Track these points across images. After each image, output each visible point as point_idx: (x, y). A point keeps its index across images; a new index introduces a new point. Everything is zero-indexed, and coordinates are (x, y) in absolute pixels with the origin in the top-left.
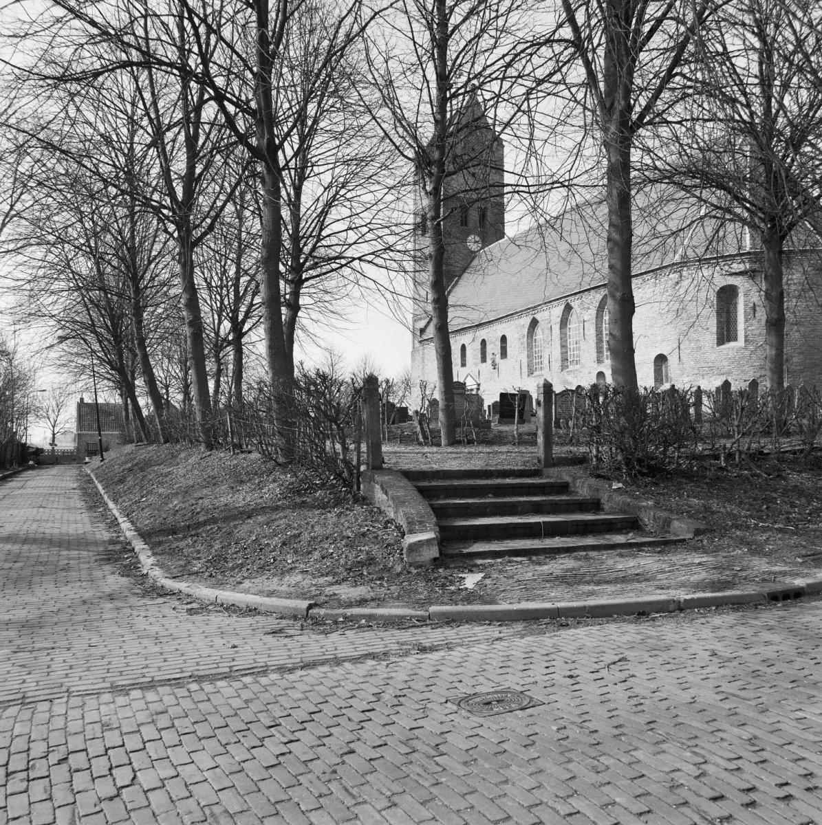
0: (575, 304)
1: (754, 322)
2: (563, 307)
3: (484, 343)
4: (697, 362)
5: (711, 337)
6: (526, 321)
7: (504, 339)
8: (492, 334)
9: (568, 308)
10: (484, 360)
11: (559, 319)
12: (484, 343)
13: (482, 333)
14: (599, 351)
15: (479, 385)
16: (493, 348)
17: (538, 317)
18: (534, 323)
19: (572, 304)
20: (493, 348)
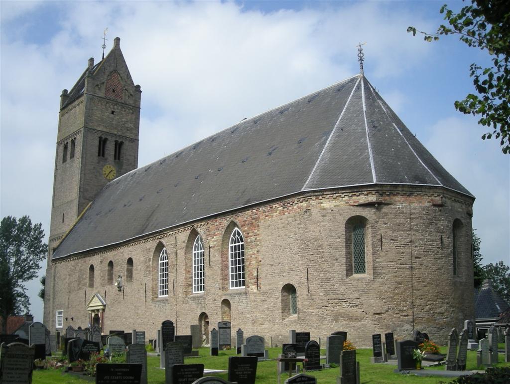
0: (201, 229)
1: (382, 254)
2: (189, 232)
3: (111, 264)
4: (327, 294)
5: (341, 267)
6: (152, 244)
7: (130, 261)
8: (120, 256)
9: (194, 233)
10: (110, 280)
11: (185, 244)
12: (111, 264)
13: (110, 255)
14: (224, 278)
15: (105, 306)
16: (121, 269)
17: (164, 241)
18: (160, 246)
19: (199, 230)
20: (121, 269)
